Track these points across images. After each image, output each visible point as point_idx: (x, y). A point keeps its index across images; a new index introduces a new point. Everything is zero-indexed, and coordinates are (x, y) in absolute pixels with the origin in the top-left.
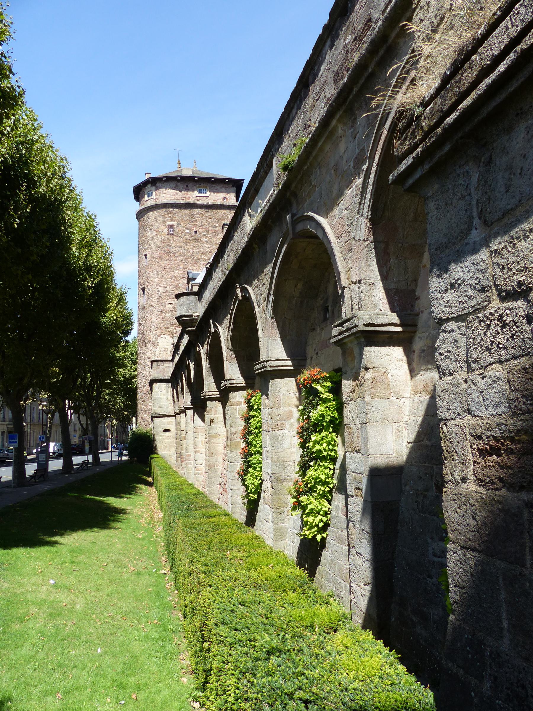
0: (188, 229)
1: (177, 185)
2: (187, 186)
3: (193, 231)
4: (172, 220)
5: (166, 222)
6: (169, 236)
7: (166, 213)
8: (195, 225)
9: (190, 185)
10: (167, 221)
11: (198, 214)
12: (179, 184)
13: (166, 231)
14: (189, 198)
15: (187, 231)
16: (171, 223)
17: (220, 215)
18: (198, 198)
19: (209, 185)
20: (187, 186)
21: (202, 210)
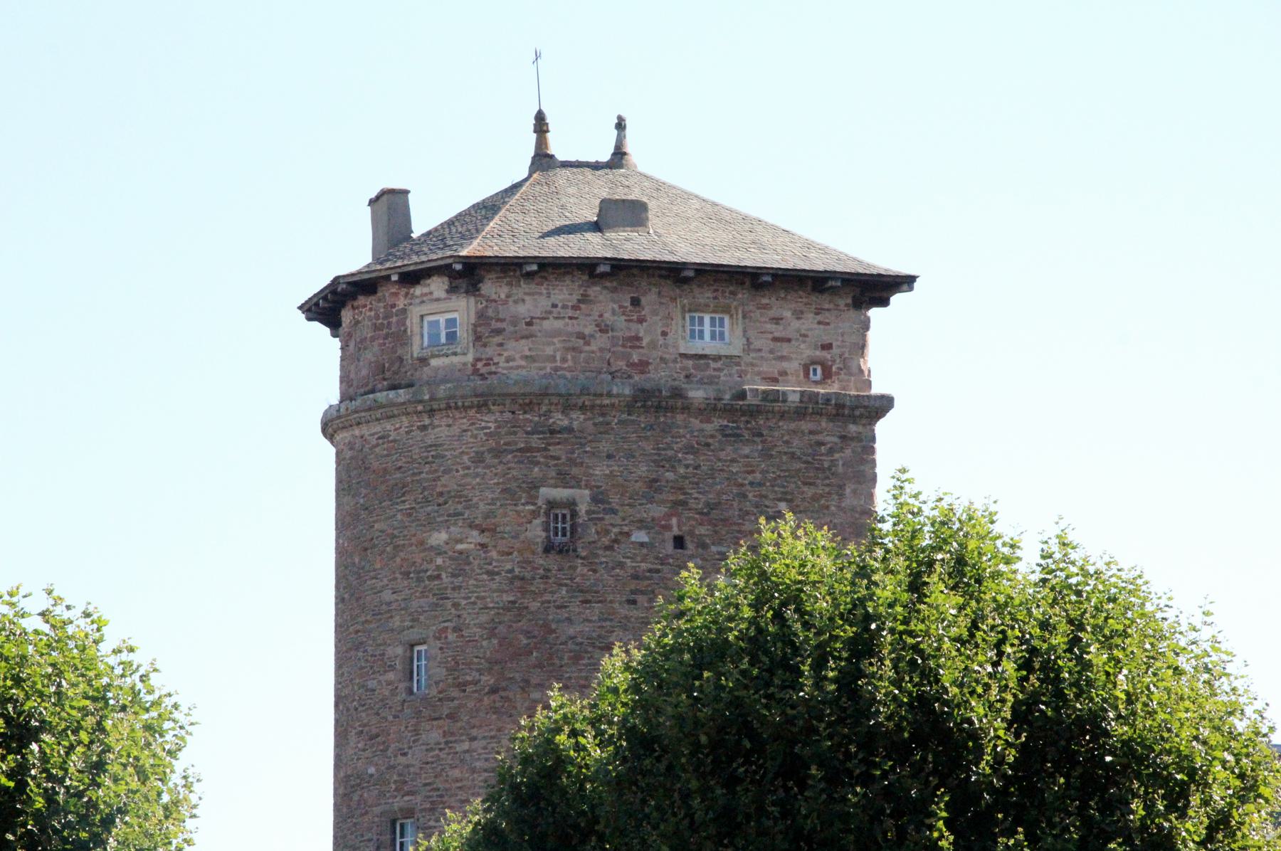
0: (642, 524)
1: (584, 299)
2: (636, 302)
3: (669, 536)
4: (564, 479)
5: (534, 486)
6: (552, 562)
7: (535, 441)
8: (677, 503)
9: (649, 299)
10: (543, 482)
11: (689, 449)
12: (595, 291)
13: (536, 532)
14: (643, 366)
15: (641, 536)
16: (561, 493)
17: (793, 456)
18: (690, 363)
19: (743, 295)
20: (636, 302)
21: (709, 428)
